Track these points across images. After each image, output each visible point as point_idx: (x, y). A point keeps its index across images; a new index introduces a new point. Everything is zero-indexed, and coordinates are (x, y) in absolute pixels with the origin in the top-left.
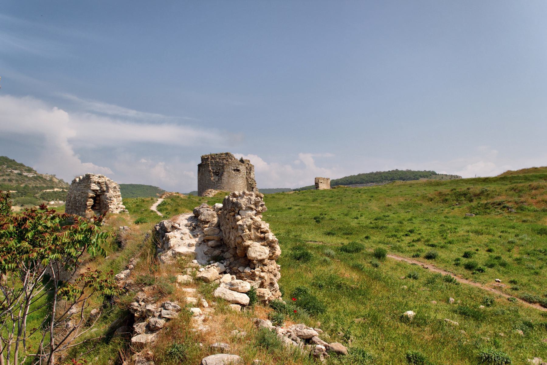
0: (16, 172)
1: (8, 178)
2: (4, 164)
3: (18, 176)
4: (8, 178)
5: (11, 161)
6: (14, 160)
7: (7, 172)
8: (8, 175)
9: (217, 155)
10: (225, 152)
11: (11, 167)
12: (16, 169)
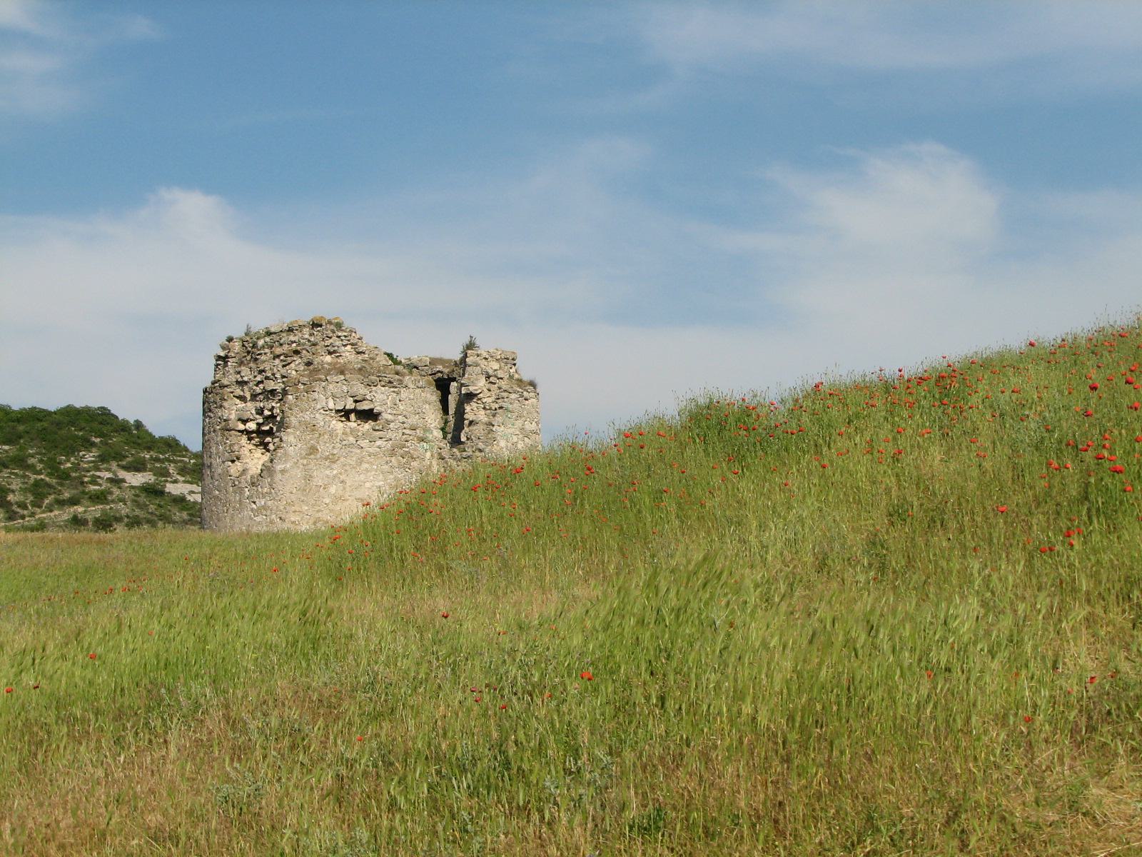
0: (136, 479)
1: (95, 511)
2: (89, 445)
3: (143, 499)
4: (95, 511)
5: (123, 427)
6: (139, 425)
7: (94, 482)
8: (100, 498)
9: (269, 334)
10: (307, 318)
11: (118, 456)
12: (138, 467)
